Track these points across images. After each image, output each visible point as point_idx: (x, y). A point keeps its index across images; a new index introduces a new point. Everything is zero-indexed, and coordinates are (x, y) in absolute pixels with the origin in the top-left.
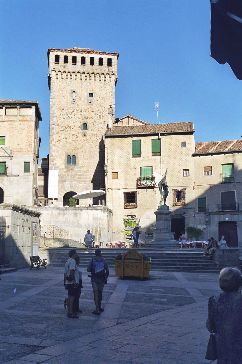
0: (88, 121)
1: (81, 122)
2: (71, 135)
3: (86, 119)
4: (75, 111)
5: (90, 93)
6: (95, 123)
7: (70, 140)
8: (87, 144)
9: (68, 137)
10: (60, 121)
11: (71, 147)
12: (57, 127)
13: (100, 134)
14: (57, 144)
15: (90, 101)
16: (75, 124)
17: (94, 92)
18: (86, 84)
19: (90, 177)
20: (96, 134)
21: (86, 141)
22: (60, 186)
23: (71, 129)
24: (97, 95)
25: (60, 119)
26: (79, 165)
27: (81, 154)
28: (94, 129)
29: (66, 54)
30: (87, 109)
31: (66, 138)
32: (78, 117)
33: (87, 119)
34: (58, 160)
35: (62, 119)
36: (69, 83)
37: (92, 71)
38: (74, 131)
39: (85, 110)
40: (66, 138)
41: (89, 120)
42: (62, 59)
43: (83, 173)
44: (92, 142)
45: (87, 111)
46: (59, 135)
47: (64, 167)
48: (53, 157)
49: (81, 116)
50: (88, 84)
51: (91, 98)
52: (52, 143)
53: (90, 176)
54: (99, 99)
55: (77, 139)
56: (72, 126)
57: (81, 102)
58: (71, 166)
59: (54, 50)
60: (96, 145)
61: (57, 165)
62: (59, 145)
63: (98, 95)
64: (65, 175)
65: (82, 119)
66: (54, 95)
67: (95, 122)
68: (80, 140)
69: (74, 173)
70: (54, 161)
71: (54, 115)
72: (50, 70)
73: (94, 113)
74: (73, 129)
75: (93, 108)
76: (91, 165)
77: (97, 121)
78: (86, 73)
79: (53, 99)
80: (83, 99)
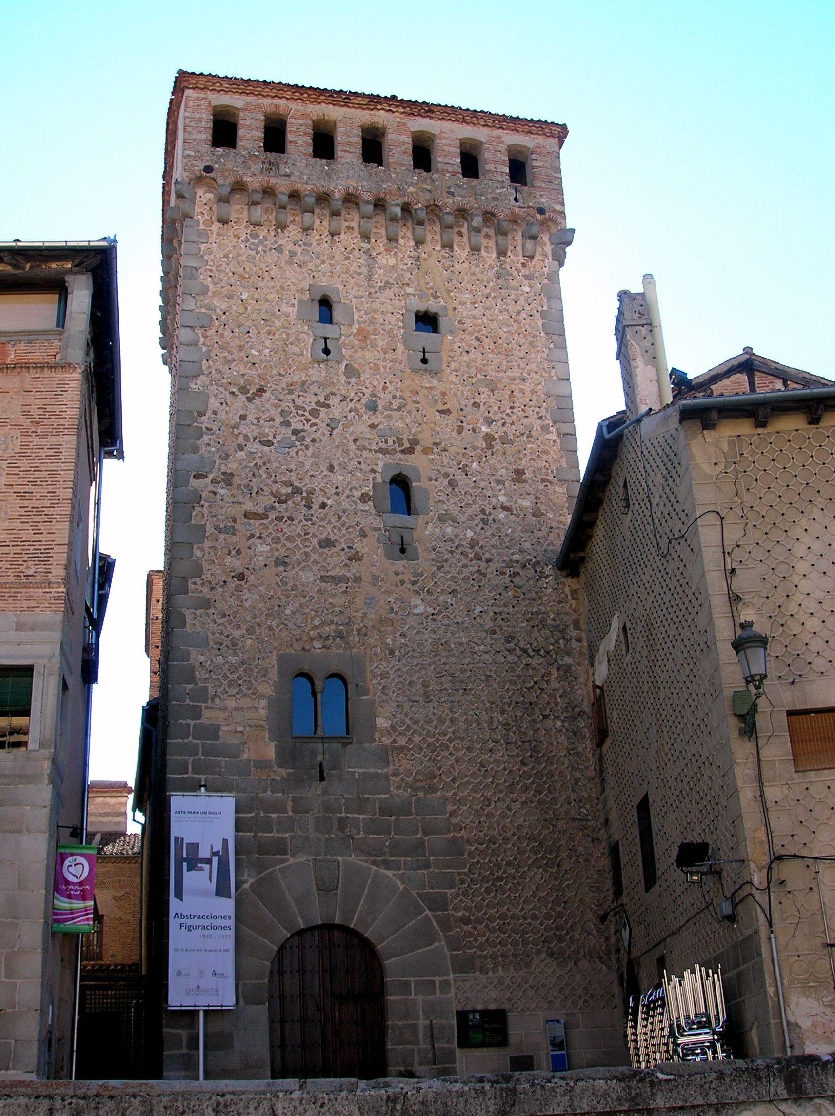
0: (420, 466)
1: (373, 471)
2: (315, 542)
3: (403, 451)
4: (334, 401)
5: (422, 307)
6: (460, 477)
7: (309, 577)
8: (420, 607)
9: (298, 556)
10: (241, 455)
11: (317, 622)
13: (493, 541)
15: (424, 352)
16: (339, 478)
17: (445, 307)
18: (392, 261)
19: (454, 821)
20: (473, 544)
21: (414, 583)
22: (246, 886)
23: (316, 506)
25: (241, 448)
26: (377, 736)
28: (455, 511)
30: (407, 394)
31: (281, 562)
32: (355, 441)
33: (410, 451)
34: (231, 703)
35: (255, 447)
36: (299, 250)
37: (428, 196)
39: (396, 404)
40: (285, 564)
43: (399, 794)
44: (454, 592)
45: (411, 406)
47: (270, 751)
48: (192, 680)
49: (368, 433)
50: (409, 261)
51: (426, 338)
52: (186, 592)
56: (317, 493)
60: (478, 609)
61: (226, 737)
62: (232, 601)
63: (468, 321)
64: (278, 807)
65: (381, 450)
66: (203, 310)
68: (375, 579)
70: (206, 714)
71: (205, 421)
75: (444, 394)
77: (475, 465)
79: (199, 332)
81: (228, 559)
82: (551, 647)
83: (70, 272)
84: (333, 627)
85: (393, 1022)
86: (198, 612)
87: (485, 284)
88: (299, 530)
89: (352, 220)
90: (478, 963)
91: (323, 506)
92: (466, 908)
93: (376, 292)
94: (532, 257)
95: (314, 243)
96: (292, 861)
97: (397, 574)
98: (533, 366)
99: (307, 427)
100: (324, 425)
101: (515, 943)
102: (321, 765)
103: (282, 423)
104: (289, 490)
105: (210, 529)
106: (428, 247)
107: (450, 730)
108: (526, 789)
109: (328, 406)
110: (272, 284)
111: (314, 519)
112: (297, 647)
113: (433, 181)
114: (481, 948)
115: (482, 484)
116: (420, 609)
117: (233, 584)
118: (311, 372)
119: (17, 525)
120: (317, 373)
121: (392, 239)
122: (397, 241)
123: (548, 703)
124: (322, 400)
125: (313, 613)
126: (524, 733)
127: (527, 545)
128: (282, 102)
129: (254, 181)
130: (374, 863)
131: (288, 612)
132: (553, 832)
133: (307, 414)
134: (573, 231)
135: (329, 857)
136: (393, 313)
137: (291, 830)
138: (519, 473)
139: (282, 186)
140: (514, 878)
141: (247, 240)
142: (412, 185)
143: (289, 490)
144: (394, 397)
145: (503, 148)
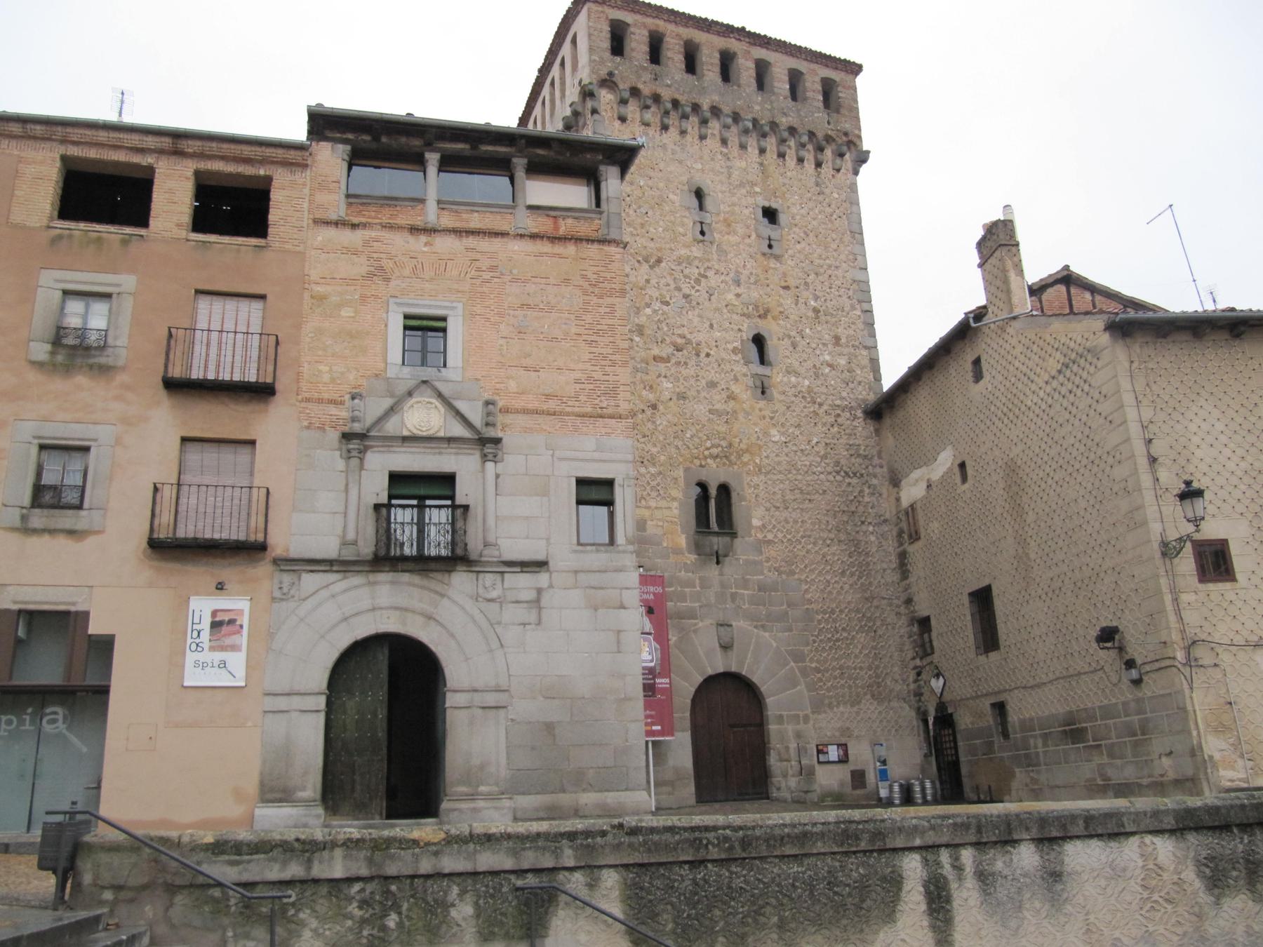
2: (704, 382)
4: (710, 274)
5: (767, 204)
7: (701, 409)
10: (648, 311)
11: (708, 444)
12: (637, 339)
18: (743, 164)
23: (703, 355)
25: (648, 305)
26: (753, 532)
29: (657, 25)
35: (657, 306)
38: (715, 366)
39: (752, 280)
47: (682, 541)
53: (806, 591)
56: (703, 344)
57: (733, 239)
60: (815, 440)
62: (649, 425)
65: (743, 315)
67: (801, 333)
76: (803, 537)
81: (644, 393)
83: (601, 162)
85: (774, 742)
88: (692, 373)
90: (827, 701)
91: (708, 355)
92: (818, 661)
94: (838, 171)
96: (701, 624)
98: (843, 257)
101: (850, 687)
108: (852, 574)
109: (706, 277)
112: (697, 462)
113: (772, 102)
114: (828, 690)
115: (814, 345)
116: (776, 439)
117: (649, 412)
118: (694, 249)
119: (588, 366)
121: (743, 147)
127: (844, 394)
128: (661, 23)
129: (646, 90)
130: (756, 627)
134: (868, 152)
137: (699, 601)
145: (818, 79)
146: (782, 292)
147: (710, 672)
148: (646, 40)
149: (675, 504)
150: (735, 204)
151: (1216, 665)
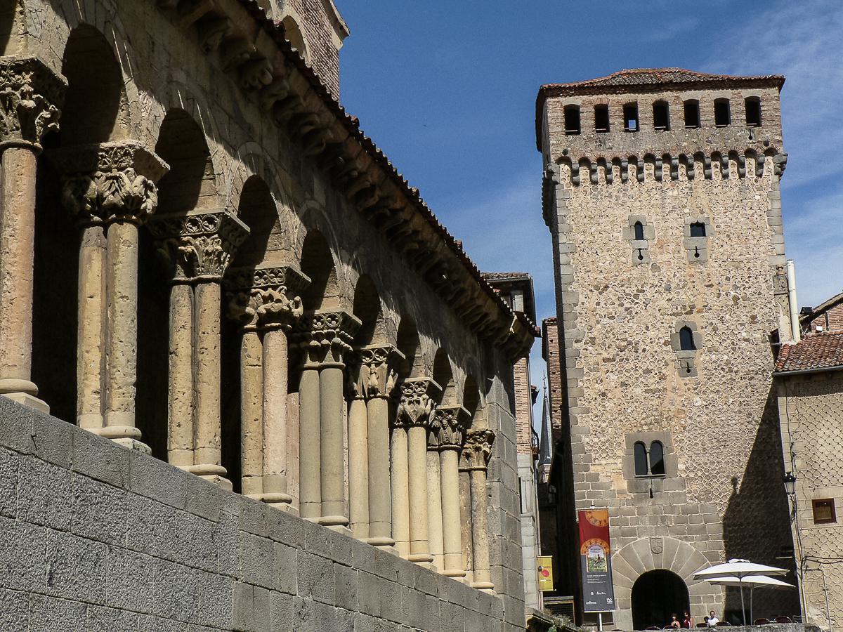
0: (696, 320)
1: (670, 327)
2: (641, 371)
3: (686, 313)
4: (646, 288)
7: (638, 391)
8: (699, 402)
10: (599, 326)
11: (644, 416)
12: (590, 348)
13: (739, 360)
14: (596, 407)
15: (696, 250)
16: (651, 334)
18: (676, 192)
20: (728, 362)
21: (695, 389)
23: (640, 351)
24: (718, 227)
25: (598, 322)
27: (681, 436)
31: (623, 384)
32: (659, 310)
33: (691, 312)
34: (603, 462)
37: (695, 146)
41: (698, 316)
42: (587, 120)
45: (690, 285)
46: (601, 374)
47: (625, 485)
52: (577, 405)
54: (726, 239)
55: (663, 384)
57: (666, 257)
58: (649, 480)
59: (556, 91)
60: (731, 400)
61: (602, 479)
63: (722, 225)
65: (673, 314)
67: (722, 320)
68: (674, 388)
69: (660, 503)
70: (592, 468)
72: (553, 158)
73: (713, 289)
74: (644, 350)
75: (708, 274)
76: (718, 473)
77: (727, 316)
78: (675, 155)
79: (570, 256)
80: (672, 247)
82: (772, 418)
84: (653, 417)
86: (584, 415)
87: (732, 198)
89: (651, 169)
91: (644, 350)
93: (667, 215)
95: (629, 189)
96: (639, 539)
97: (686, 384)
99: (633, 305)
100: (641, 303)
102: (651, 490)
103: (619, 305)
104: (625, 343)
105: (586, 370)
106: (696, 180)
107: (717, 468)
108: (759, 496)
109: (644, 291)
110: (607, 219)
111: (640, 358)
112: (635, 430)
115: (732, 327)
120: (636, 272)
122: (678, 178)
123: (771, 450)
124: (640, 288)
125: (642, 411)
126: (758, 467)
127: (758, 361)
131: (629, 411)
132: (774, 519)
133: (632, 297)
135: (657, 537)
136: (676, 227)
138: (754, 317)
139: (608, 156)
140: (753, 544)
141: (591, 193)
142: (685, 141)
143: (625, 343)
144: (680, 281)
145: (742, 101)
146: (706, 290)
147: (645, 570)
148: (592, 115)
149: (620, 460)
150: (668, 228)
151: (818, 569)
